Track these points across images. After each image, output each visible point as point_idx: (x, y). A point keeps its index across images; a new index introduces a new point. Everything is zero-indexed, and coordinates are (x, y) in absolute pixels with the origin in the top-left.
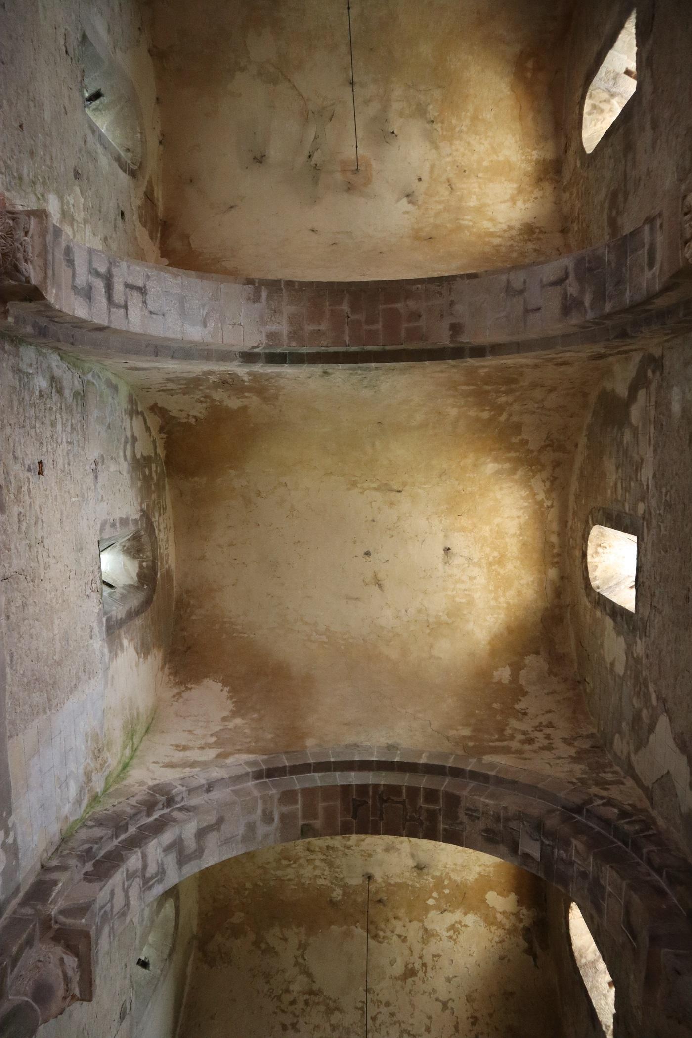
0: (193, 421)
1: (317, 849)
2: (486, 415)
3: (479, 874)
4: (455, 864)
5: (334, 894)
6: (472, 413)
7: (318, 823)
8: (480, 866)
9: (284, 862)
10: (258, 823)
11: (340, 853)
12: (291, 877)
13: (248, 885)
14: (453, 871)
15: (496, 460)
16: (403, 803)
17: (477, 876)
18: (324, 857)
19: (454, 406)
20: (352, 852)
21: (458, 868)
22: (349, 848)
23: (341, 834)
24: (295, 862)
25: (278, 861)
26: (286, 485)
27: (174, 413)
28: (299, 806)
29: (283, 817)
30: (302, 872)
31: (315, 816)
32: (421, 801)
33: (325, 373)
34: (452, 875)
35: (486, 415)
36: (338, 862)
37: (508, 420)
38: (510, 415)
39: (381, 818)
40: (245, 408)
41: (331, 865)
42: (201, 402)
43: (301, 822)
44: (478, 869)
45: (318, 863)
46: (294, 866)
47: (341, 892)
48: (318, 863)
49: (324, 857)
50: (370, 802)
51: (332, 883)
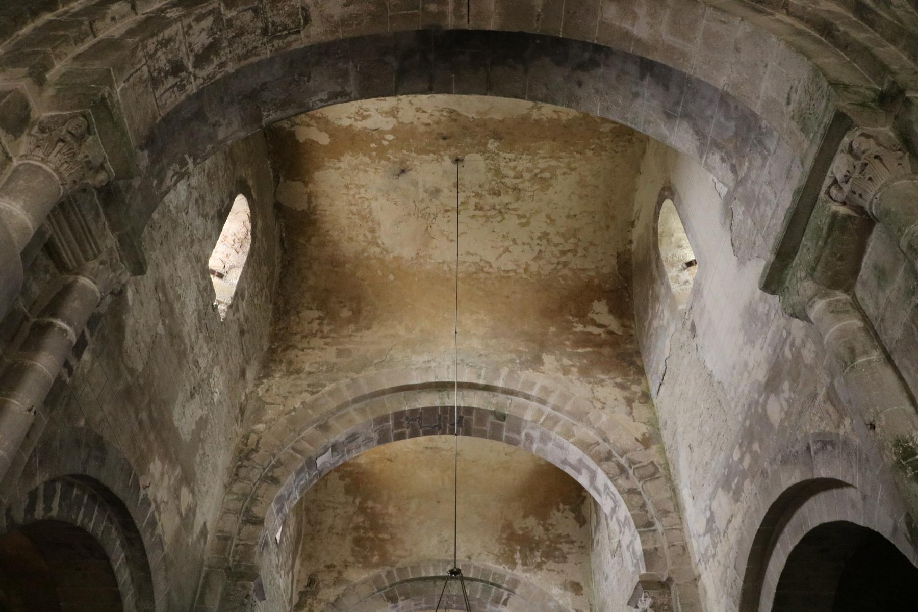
0: (561, 507)
1: (510, 191)
2: (370, 504)
3: (339, 161)
4: (366, 172)
5: (496, 144)
6: (379, 507)
7: (491, 418)
8: (339, 168)
9: (547, 175)
10: (537, 440)
11: (487, 186)
12: (540, 161)
13: (589, 153)
14: (368, 165)
15: (359, 465)
16: (421, 427)
17: (342, 158)
18: (503, 180)
19: (391, 515)
20: (473, 189)
21: (362, 167)
22: (477, 195)
23: (473, 408)
24: (536, 175)
25: (554, 176)
26: (506, 454)
27: (571, 515)
28: (505, 434)
29: (519, 433)
30: (530, 165)
31: (492, 423)
32: (408, 431)
33: (470, 558)
34: (368, 160)
35: (370, 504)
36: (490, 176)
37: (355, 498)
38: (354, 502)
39: (440, 417)
40: (525, 516)
41: (497, 172)
42: (551, 525)
43: (505, 423)
44: (341, 165)
45: (512, 174)
46: (537, 171)
47: (489, 146)
48: (512, 174)
49: (503, 180)
50: (448, 425)
51: (498, 154)
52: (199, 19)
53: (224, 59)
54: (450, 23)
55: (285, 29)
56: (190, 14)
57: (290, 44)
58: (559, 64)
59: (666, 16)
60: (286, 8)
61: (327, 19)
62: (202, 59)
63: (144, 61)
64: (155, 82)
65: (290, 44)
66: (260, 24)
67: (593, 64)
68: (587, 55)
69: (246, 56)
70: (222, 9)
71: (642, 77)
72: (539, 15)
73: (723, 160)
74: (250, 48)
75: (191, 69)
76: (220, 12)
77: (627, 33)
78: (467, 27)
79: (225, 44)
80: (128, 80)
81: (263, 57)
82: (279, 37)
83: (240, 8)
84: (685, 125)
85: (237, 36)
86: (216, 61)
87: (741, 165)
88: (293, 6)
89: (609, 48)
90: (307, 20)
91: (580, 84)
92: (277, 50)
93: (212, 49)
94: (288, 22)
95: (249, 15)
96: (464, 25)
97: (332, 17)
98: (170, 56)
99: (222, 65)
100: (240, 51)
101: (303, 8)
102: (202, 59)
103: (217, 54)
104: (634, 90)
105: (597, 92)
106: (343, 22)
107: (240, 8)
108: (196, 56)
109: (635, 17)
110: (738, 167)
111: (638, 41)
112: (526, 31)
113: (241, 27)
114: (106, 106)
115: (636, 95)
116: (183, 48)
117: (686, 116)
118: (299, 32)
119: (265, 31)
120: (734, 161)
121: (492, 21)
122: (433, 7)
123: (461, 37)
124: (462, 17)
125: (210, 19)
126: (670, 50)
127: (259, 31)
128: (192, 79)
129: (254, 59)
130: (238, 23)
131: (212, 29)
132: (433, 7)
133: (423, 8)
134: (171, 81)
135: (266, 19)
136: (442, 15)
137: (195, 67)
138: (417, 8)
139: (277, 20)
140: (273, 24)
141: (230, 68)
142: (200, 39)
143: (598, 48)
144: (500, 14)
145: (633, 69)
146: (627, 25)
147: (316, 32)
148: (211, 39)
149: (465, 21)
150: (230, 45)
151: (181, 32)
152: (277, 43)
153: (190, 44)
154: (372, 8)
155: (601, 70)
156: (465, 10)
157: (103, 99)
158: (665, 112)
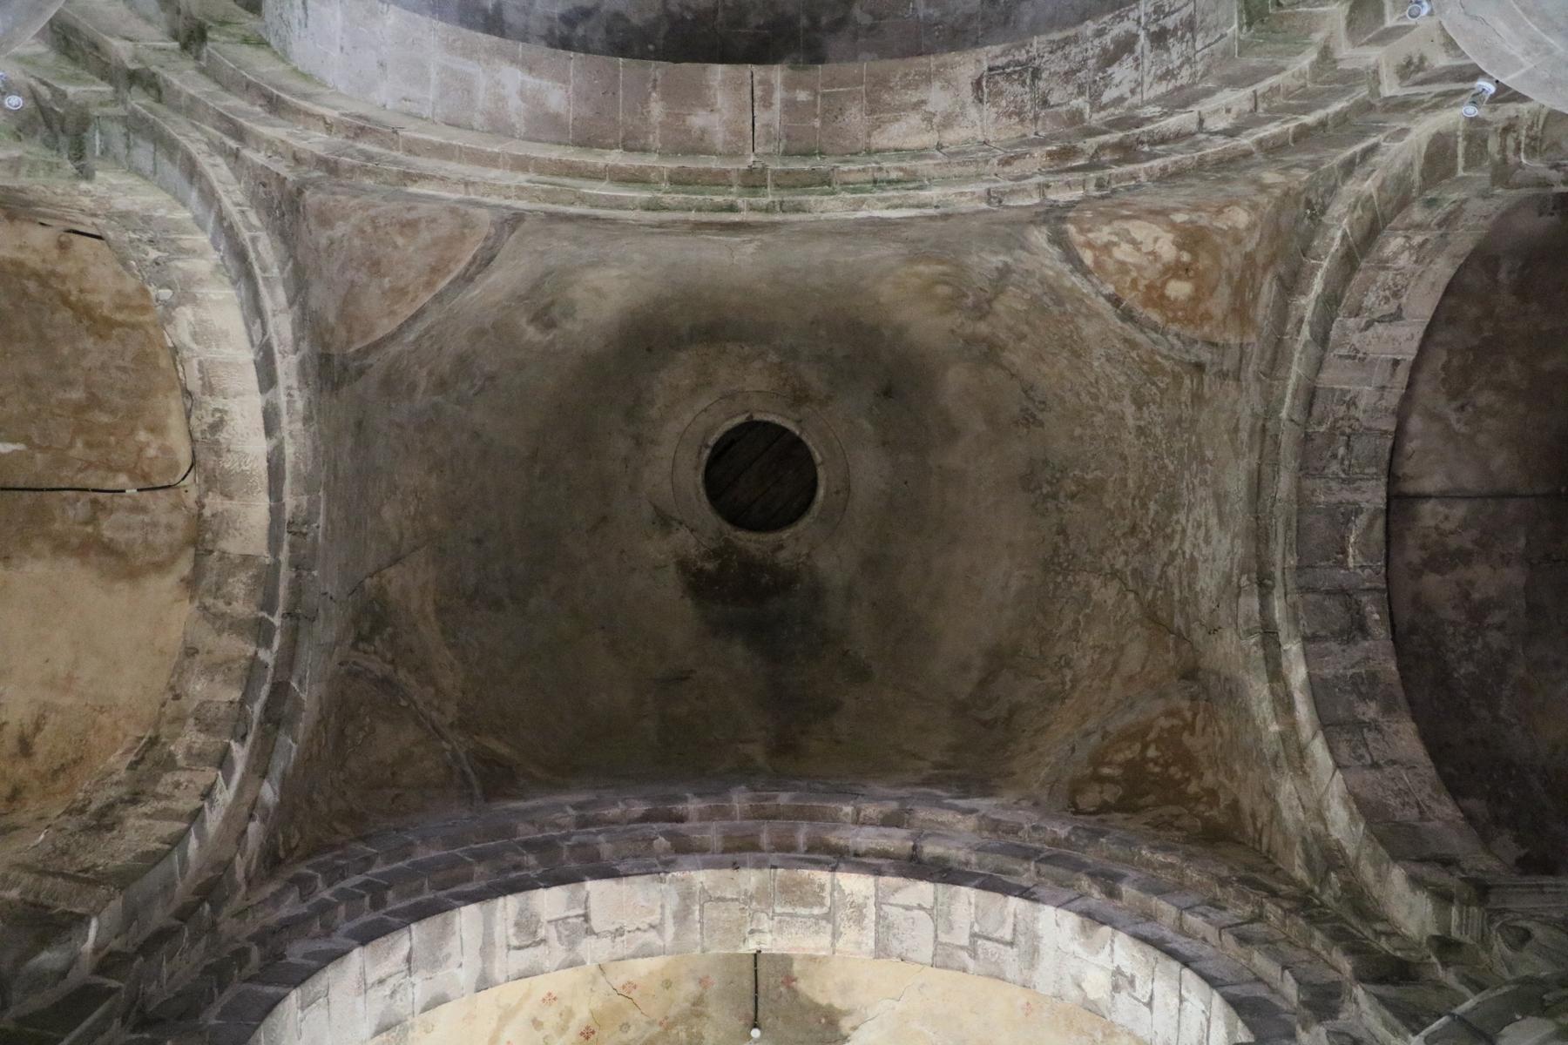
52: (1120, 100)
53: (1096, 42)
54: (777, 74)
55: (1009, 75)
56: (1129, 108)
57: (1003, 54)
58: (618, 16)
59: (482, 97)
60: (1004, 103)
61: (949, 84)
62: (1126, 45)
63: (1198, 56)
64: (1190, 25)
65: (1003, 54)
66: (1042, 84)
67: (569, 20)
68: (580, 31)
69: (1067, 41)
70: (1088, 110)
72: (654, 87)
74: (1060, 53)
75: (1142, 34)
76: (1092, 105)
77: (531, 69)
78: (754, 68)
79: (1091, 62)
80: (1222, 36)
81: (1043, 38)
82: (1018, 63)
83: (1065, 108)
85: (1074, 72)
86: (1107, 39)
88: (994, 105)
89: (551, 45)
90: (977, 85)
92: (1024, 46)
93: (1109, 58)
94: (1003, 85)
95: (1053, 99)
96: (759, 71)
97: (942, 88)
98: (1165, 56)
99: (1100, 33)
100: (1073, 50)
101: (981, 101)
102: (1126, 45)
103: (1104, 50)
106: (928, 79)
107: (1065, 108)
108: (1132, 51)
109: (522, 93)
111: (513, 61)
112: (671, 65)
113: (1067, 82)
114: (1249, 13)
116: (1147, 63)
118: (990, 69)
119: (1036, 74)
121: (719, 77)
122: (802, 96)
123: (760, 51)
124: (760, 83)
125: (1105, 99)
126: (469, 53)
127: (1044, 75)
128: (1143, 20)
129: (1056, 36)
130: (1070, 88)
131: (1106, 86)
132: (802, 96)
133: (816, 93)
134: (1170, 22)
135: (1032, 90)
136: (790, 85)
137: (1137, 36)
138: (824, 95)
139: (1017, 88)
140: (1023, 84)
141: (1090, 27)
142: (1122, 72)
143: (565, 44)
144: (708, 87)
145: (511, 16)
146: (532, 81)
147: (967, 66)
148: (1110, 71)
149: (756, 77)
150: (1085, 60)
151: (1146, 86)
152: (1022, 56)
153: (1137, 68)
154: (886, 97)
156: (758, 93)
157: (1250, 24)
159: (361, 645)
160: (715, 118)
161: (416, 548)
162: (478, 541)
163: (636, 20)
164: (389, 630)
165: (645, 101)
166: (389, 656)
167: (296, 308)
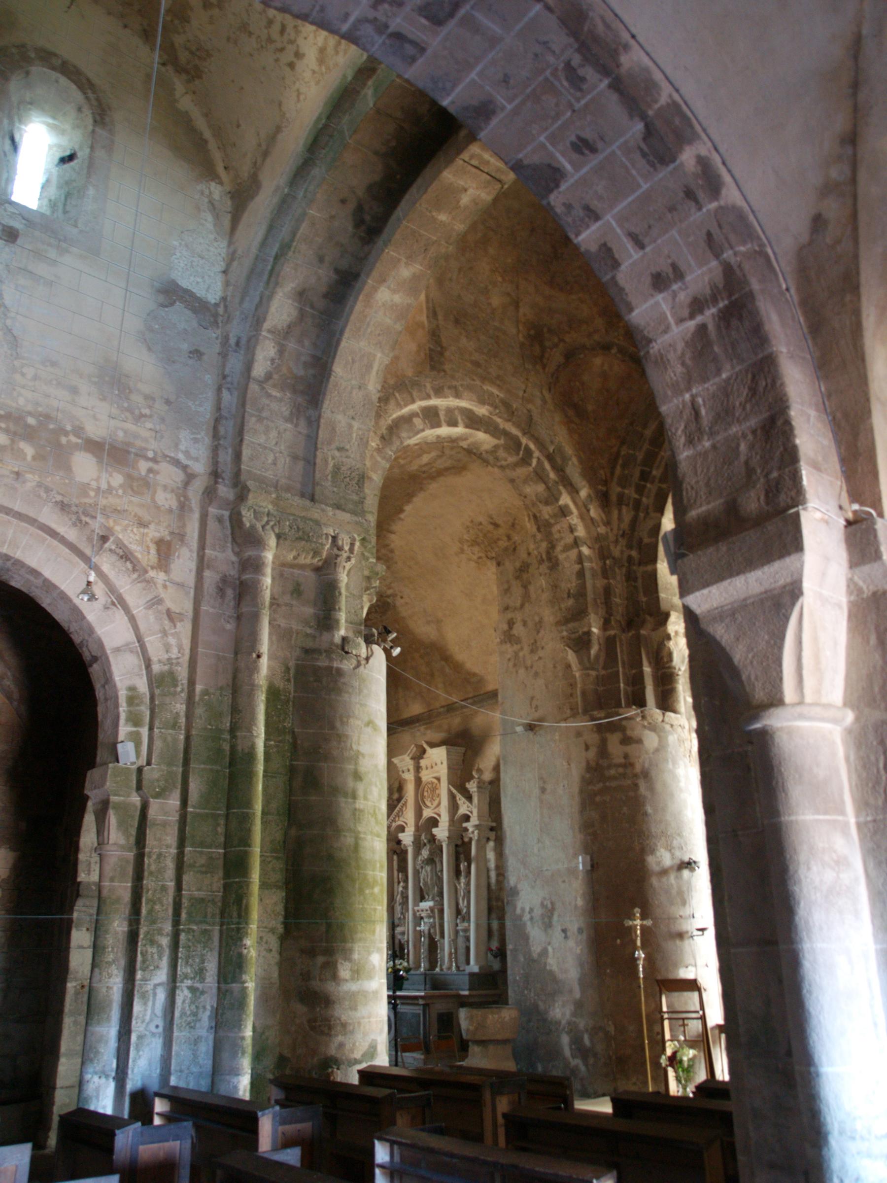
58: (370, 188)
67: (359, 222)
71: (337, 271)
72: (430, 212)
73: (273, 360)
77: (384, 281)
78: (462, 156)
84: (295, 313)
87: (274, 386)
91: (343, 201)
104: (327, 259)
105: (332, 217)
109: (394, 292)
110: (271, 382)
111: (375, 289)
115: (321, 260)
117: (302, 314)
120: (276, 376)
144: (451, 184)
149: (467, 159)
155: (350, 228)
158: (304, 290)
159: (545, 361)
160: (471, 191)
161: (517, 287)
162: (533, 230)
163: (377, 178)
164: (545, 330)
165: (434, 219)
166: (556, 340)
167: (415, 394)
